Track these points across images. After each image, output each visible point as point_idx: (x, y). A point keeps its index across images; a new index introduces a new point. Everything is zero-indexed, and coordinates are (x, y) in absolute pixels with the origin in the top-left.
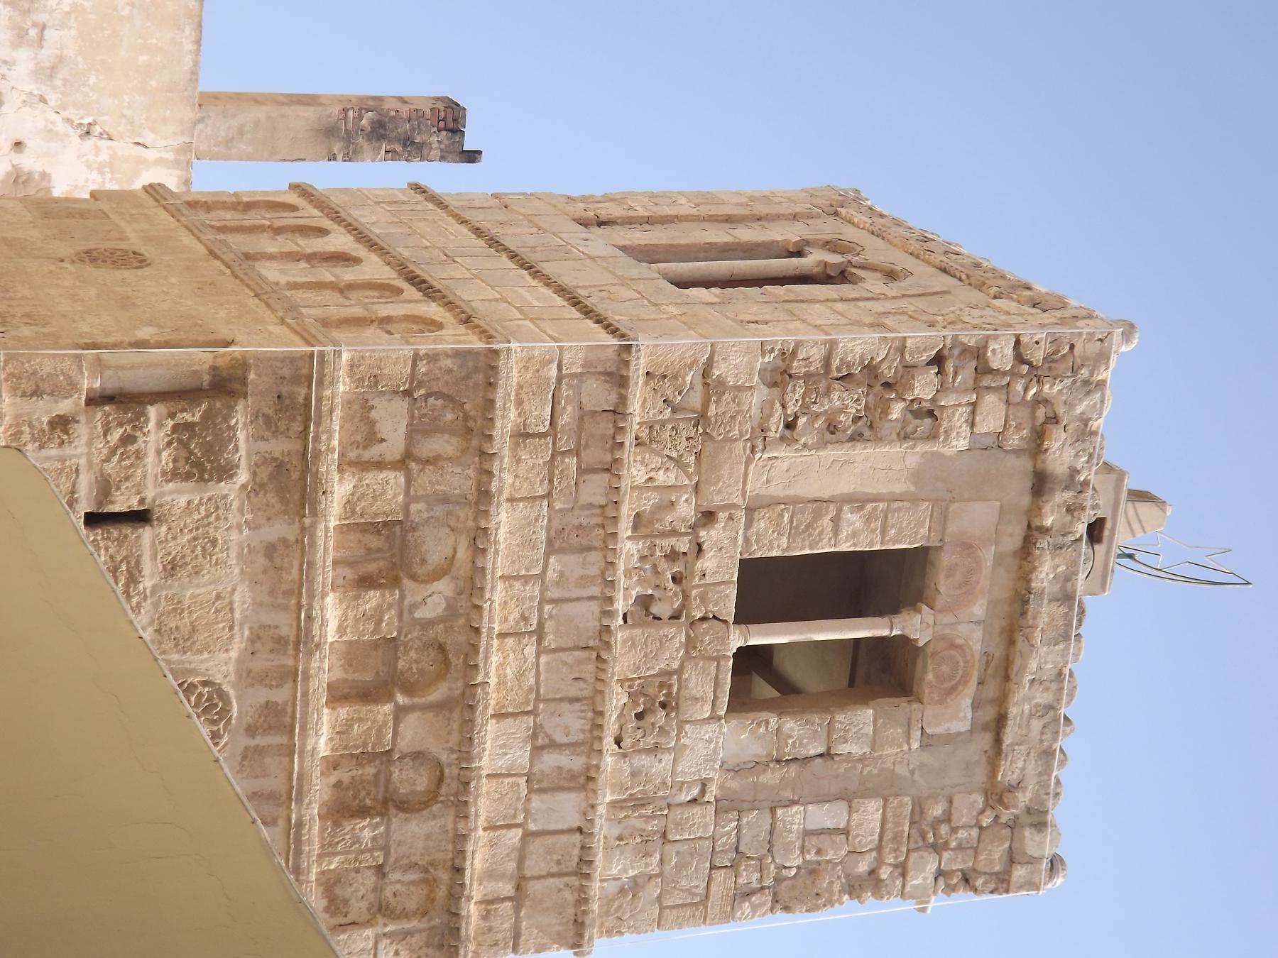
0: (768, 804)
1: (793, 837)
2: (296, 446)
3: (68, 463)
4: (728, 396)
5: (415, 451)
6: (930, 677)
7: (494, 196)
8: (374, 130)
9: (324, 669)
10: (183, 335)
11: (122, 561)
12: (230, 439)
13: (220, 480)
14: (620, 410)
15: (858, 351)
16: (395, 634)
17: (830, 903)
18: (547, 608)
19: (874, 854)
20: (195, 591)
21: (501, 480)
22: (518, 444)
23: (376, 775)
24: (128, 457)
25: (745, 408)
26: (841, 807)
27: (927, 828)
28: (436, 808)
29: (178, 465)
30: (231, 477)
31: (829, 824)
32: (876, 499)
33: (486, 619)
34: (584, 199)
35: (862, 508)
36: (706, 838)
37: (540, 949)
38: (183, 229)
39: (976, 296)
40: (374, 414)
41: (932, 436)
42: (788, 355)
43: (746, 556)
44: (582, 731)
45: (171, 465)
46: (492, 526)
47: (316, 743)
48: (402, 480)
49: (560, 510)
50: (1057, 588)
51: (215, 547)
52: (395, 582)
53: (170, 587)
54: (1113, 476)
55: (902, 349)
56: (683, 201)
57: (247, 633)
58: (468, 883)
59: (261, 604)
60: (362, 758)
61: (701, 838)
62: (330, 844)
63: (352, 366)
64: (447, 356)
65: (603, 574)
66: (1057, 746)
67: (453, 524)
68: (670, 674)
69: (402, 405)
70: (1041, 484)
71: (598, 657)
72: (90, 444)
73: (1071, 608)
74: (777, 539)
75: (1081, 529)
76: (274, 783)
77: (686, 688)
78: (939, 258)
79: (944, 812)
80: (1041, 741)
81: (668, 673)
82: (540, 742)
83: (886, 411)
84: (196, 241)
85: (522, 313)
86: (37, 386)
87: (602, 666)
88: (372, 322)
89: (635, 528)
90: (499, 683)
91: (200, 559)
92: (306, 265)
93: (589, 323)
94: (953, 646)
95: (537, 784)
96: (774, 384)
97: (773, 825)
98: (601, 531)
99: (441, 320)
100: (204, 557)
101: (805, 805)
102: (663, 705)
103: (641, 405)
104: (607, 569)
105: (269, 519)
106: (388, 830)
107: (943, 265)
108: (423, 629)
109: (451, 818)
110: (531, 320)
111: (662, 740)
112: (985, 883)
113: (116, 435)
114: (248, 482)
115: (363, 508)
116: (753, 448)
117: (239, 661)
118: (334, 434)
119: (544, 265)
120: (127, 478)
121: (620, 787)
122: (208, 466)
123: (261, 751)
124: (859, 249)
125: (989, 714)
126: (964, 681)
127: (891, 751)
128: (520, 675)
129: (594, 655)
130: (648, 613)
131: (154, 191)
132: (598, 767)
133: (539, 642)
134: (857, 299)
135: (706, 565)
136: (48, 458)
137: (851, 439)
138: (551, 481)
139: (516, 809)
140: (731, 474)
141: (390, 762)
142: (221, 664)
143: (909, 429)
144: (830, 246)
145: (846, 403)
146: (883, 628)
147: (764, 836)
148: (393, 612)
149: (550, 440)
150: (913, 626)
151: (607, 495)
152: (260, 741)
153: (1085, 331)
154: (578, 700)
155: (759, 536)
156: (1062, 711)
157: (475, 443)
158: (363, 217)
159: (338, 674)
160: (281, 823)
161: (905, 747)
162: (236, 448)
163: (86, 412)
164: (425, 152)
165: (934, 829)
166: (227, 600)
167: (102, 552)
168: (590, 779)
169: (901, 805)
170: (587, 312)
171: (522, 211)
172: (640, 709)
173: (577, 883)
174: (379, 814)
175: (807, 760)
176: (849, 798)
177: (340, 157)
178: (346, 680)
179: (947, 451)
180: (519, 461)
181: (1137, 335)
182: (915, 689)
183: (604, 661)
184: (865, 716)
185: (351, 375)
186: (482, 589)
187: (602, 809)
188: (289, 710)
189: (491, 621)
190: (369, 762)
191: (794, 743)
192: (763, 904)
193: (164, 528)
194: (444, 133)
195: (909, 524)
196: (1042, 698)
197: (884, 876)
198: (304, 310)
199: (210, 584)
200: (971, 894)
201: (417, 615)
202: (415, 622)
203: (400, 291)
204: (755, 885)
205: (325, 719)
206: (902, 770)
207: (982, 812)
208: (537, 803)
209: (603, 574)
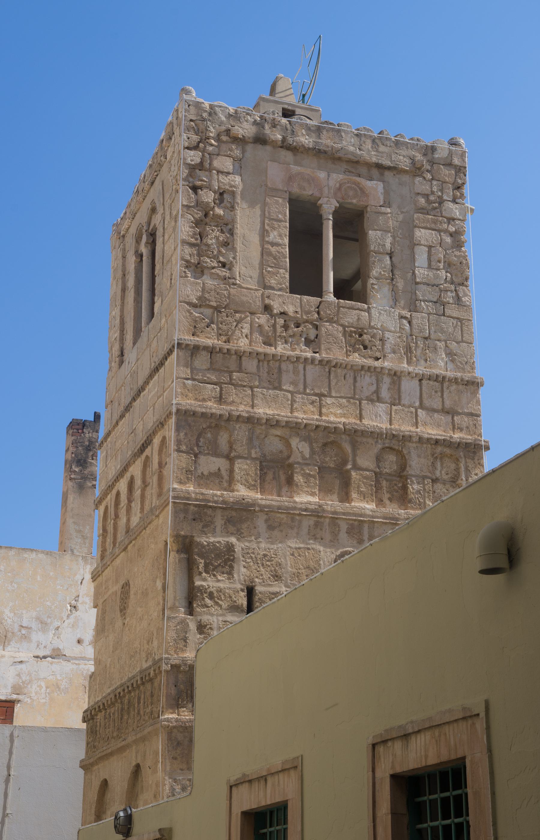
1: (431, 274)
2: (219, 513)
3: (221, 626)
4: (207, 295)
5: (225, 453)
6: (354, 201)
8: (81, 465)
9: (332, 504)
10: (161, 566)
12: (215, 545)
13: (234, 551)
14: (210, 350)
15: (188, 229)
17: (465, 257)
19: (442, 234)
20: (289, 565)
21: (242, 411)
22: (225, 402)
23: (387, 480)
24: (220, 596)
25: (213, 287)
26: (417, 249)
27: (431, 206)
28: (405, 452)
31: (425, 256)
32: (263, 223)
33: (311, 422)
34: (110, 362)
35: (267, 231)
36: (429, 317)
37: (478, 402)
38: (113, 563)
39: (165, 168)
40: (206, 473)
41: (233, 194)
42: (188, 265)
43: (288, 290)
44: (371, 376)
45: (225, 575)
46: (265, 417)
47: (369, 509)
48: (239, 461)
49: (259, 382)
50: (313, 134)
51: (267, 555)
52: (291, 466)
53: (286, 578)
54: (262, 103)
57: (311, 541)
58: (443, 438)
59: (298, 534)
60: (378, 487)
61: (428, 320)
63: (180, 483)
64: (178, 435)
65: (293, 362)
66: (393, 139)
67: (263, 436)
68: (345, 331)
69: (202, 459)
71: (334, 367)
72: (212, 615)
73: (324, 128)
75: (284, 121)
77: (352, 323)
78: (146, 186)
79: (423, 197)
80: (390, 146)
81: (344, 333)
82: (375, 398)
83: (219, 216)
84: (119, 557)
86: (182, 639)
87: (339, 366)
88: (160, 472)
89: (271, 345)
90: (344, 417)
92: (133, 503)
94: (339, 189)
95: (396, 401)
96: (202, 273)
97: (425, 284)
98: (271, 362)
99: (161, 437)
100: (272, 561)
101: (415, 267)
102: (361, 335)
104: (290, 360)
105: (255, 528)
106: (414, 476)
107: (150, 184)
108: (315, 454)
109: (410, 444)
110: (164, 392)
112: (460, 179)
113: (208, 601)
114: (236, 537)
115: (253, 480)
116: (234, 284)
117: (325, 546)
118: (214, 493)
119: (139, 384)
120: (230, 597)
121: (400, 359)
124: (140, 226)
125: (375, 172)
126: (358, 184)
127: (391, 223)
128: (341, 406)
129: (333, 369)
130: (313, 341)
131: (95, 577)
132: (389, 370)
134: (164, 228)
135: (291, 311)
137: (232, 235)
138: (244, 386)
139: (408, 412)
140: (246, 296)
141: (381, 473)
143: (229, 205)
144: (138, 241)
145: (214, 236)
146: (328, 224)
147: (429, 289)
148: (305, 468)
150: (328, 207)
153: (184, 114)
156: (376, 135)
157: (223, 423)
158: (112, 473)
159: (335, 497)
161: (389, 215)
163: (196, 616)
164: (93, 440)
165: (432, 203)
166: (294, 550)
168: (395, 374)
169: (418, 219)
171: (114, 394)
172: (362, 347)
173: (447, 383)
174: (406, 480)
175: (393, 265)
176: (413, 245)
177: (94, 483)
178: (338, 494)
179: (241, 187)
180: (233, 402)
181: (188, 87)
183: (336, 364)
184: (372, 234)
186: (296, 423)
187: (411, 369)
188: (351, 522)
189: (313, 419)
190: (380, 484)
191: (384, 271)
192: (464, 290)
193: (256, 580)
194: (85, 430)
195: (277, 208)
196: (368, 145)
197: (454, 229)
198: (153, 505)
199: (286, 558)
201: (308, 456)
203: (147, 457)
204: (454, 294)
206: (401, 217)
207: (424, 178)
208: (406, 401)
209: (293, 362)
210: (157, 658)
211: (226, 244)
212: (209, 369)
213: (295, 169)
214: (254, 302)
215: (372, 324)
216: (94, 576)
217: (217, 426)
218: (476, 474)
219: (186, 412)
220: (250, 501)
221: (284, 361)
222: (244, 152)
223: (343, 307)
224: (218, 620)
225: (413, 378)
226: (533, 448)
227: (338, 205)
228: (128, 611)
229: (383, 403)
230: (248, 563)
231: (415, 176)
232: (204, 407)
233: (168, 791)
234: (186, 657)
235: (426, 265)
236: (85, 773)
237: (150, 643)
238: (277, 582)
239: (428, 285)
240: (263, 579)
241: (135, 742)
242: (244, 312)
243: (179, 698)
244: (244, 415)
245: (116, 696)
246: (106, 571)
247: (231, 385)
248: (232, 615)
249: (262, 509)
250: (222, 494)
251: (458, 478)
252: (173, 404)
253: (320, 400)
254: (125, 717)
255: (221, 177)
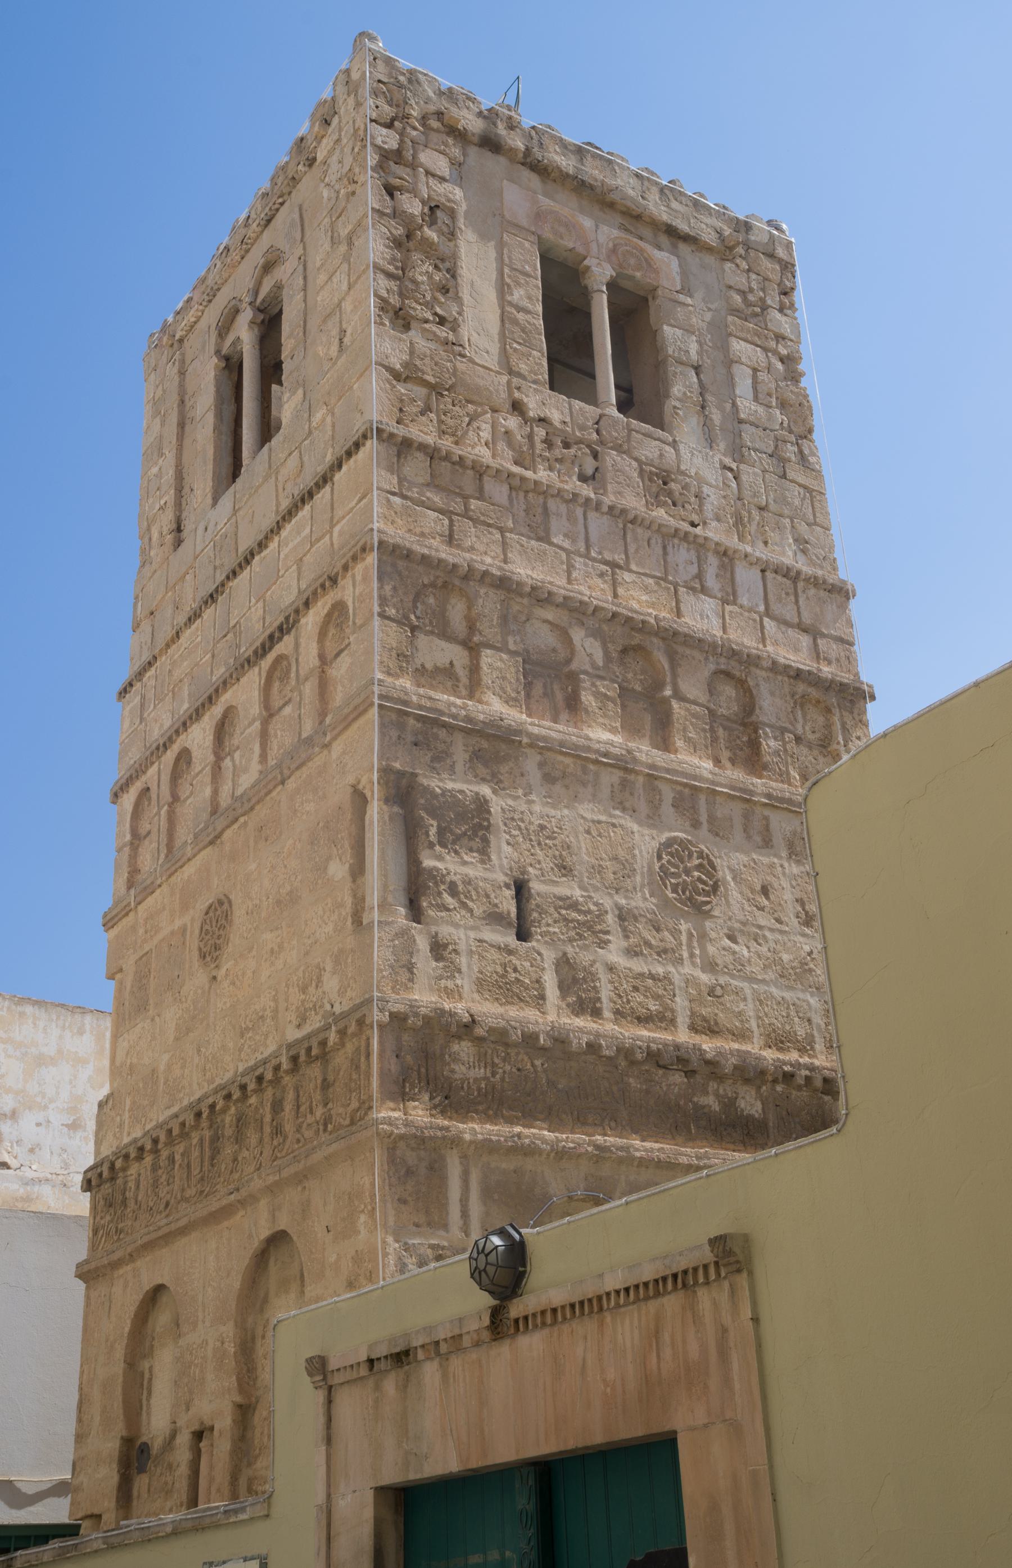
0: (736, 423)
1: (761, 410)
2: (459, 739)
3: (474, 949)
4: (418, 363)
6: (638, 274)
7: (136, 627)
9: (645, 751)
11: (559, 913)
12: (453, 796)
13: (489, 812)
14: (430, 451)
15: (382, 248)
16: (616, 686)
17: (806, 396)
18: (593, 554)
20: (584, 853)
21: (490, 565)
23: (725, 729)
24: (469, 892)
26: (736, 369)
28: (751, 684)
29: (475, 848)
30: (486, 801)
31: (749, 381)
33: (605, 605)
35: (509, 286)
36: (764, 476)
37: (850, 624)
38: (173, 879)
40: (429, 666)
41: (452, 214)
43: (547, 386)
45: (475, 854)
46: (530, 582)
47: (706, 769)
48: (488, 651)
49: (513, 523)
50: (572, 157)
51: (546, 828)
52: (573, 678)
53: (581, 873)
55: (380, 213)
56: (155, 470)
57: (618, 812)
59: (594, 795)
62: (781, 775)
63: (389, 674)
65: (567, 502)
67: (524, 618)
70: (490, 144)
71: (631, 522)
72: (457, 926)
73: (588, 151)
74: (534, 358)
76: (736, 810)
77: (652, 460)
81: (641, 473)
82: (698, 586)
83: (431, 244)
84: (192, 863)
85: (318, 540)
88: (323, 672)
91: (556, 842)
93: (338, 477)
94: (614, 251)
96: (407, 327)
97: (752, 424)
98: (531, 495)
100: (555, 838)
101: (735, 396)
102: (665, 483)
103: (423, 431)
104: (562, 497)
105: (522, 775)
106: (770, 726)
107: (263, 223)
108: (612, 662)
109: (758, 672)
110: (332, 527)
111: (693, 490)
113: (449, 900)
114: (491, 787)
115: (513, 690)
117: (640, 824)
119: (241, 550)
120: (488, 896)
122: (476, 820)
123: (712, 819)
124: (233, 302)
125: (664, 240)
126: (642, 251)
128: (646, 589)
129: (629, 525)
132: (717, 544)
133: (620, 567)
136: (469, 966)
137: (454, 276)
138: (489, 525)
142: (645, 841)
145: (423, 271)
146: (602, 298)
147: (760, 432)
148: (598, 683)
149: (455, 518)
150: (600, 273)
151: (502, 482)
152: (704, 818)
154: (664, 548)
155: (530, 372)
157: (457, 582)
159: (647, 741)
160: (767, 812)
161: (690, 308)
162: (461, 792)
163: (427, 924)
166: (591, 824)
167: (551, 929)
168: (725, 553)
169: (734, 324)
170: (325, 479)
171: (159, 597)
172: (670, 502)
174: (756, 731)
176: (730, 362)
178: (651, 737)
182: (642, 293)
183: (636, 517)
185: (397, 676)
186: (581, 602)
187: (749, 549)
188: (679, 788)
191: (690, 392)
193: (530, 869)
196: (654, 196)
199: (577, 836)
200: (796, 293)
201: (601, 664)
202: (606, 667)
205: (688, 758)
206: (708, 316)
207: (737, 265)
208: (744, 600)
210: (338, 1009)
211: (443, 291)
212: (428, 485)
213: (545, 202)
214: (497, 391)
215: (683, 467)
216: (109, 921)
217: (445, 585)
218: (859, 738)
219: (396, 547)
220: (513, 723)
221: (552, 496)
222: (465, 155)
223: (637, 432)
224: (467, 937)
225: (751, 564)
226: (977, 684)
227: (614, 274)
228: (231, 948)
229: (710, 596)
230: (515, 836)
231: (724, 260)
232: (426, 546)
233: (393, 1268)
234: (416, 1000)
235: (751, 396)
236: (87, 1288)
237: (312, 989)
238: (565, 879)
239: (757, 427)
240: (541, 869)
241: (271, 1190)
242: (480, 404)
243: (404, 1080)
244: (494, 572)
245: (198, 1115)
246: (150, 901)
247: (470, 519)
248: (493, 931)
249: (534, 739)
250: (464, 707)
251: (831, 740)
252: (372, 530)
253: (613, 574)
254: (228, 1150)
255: (431, 180)
